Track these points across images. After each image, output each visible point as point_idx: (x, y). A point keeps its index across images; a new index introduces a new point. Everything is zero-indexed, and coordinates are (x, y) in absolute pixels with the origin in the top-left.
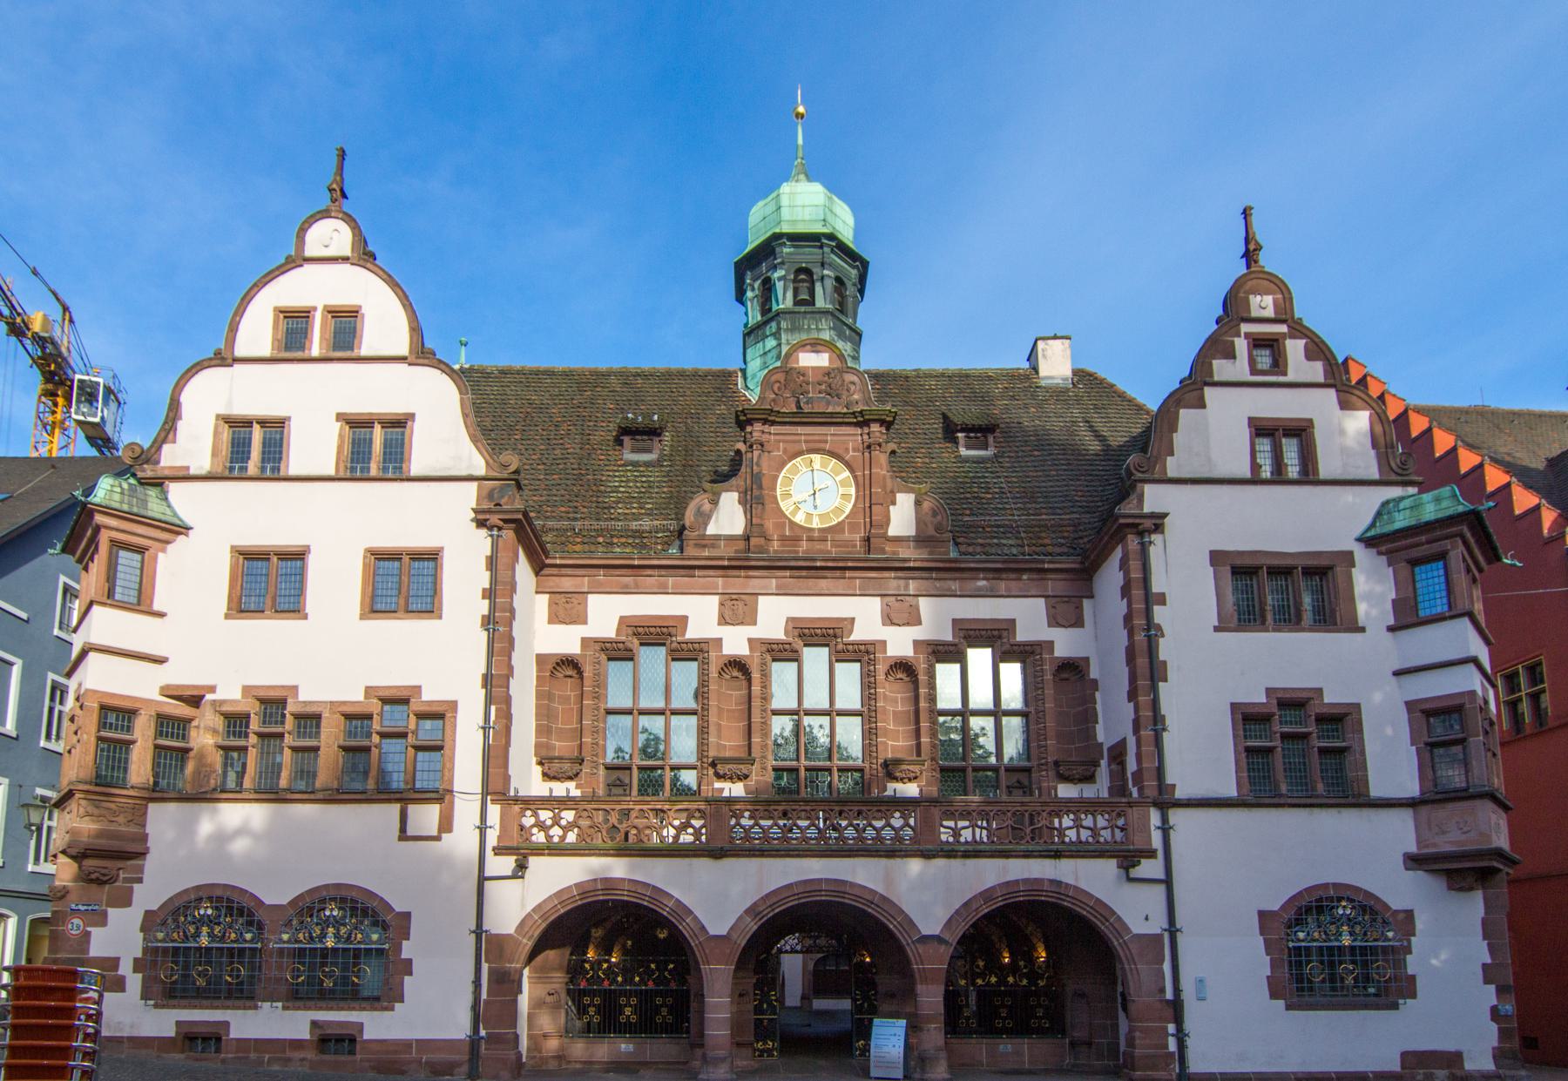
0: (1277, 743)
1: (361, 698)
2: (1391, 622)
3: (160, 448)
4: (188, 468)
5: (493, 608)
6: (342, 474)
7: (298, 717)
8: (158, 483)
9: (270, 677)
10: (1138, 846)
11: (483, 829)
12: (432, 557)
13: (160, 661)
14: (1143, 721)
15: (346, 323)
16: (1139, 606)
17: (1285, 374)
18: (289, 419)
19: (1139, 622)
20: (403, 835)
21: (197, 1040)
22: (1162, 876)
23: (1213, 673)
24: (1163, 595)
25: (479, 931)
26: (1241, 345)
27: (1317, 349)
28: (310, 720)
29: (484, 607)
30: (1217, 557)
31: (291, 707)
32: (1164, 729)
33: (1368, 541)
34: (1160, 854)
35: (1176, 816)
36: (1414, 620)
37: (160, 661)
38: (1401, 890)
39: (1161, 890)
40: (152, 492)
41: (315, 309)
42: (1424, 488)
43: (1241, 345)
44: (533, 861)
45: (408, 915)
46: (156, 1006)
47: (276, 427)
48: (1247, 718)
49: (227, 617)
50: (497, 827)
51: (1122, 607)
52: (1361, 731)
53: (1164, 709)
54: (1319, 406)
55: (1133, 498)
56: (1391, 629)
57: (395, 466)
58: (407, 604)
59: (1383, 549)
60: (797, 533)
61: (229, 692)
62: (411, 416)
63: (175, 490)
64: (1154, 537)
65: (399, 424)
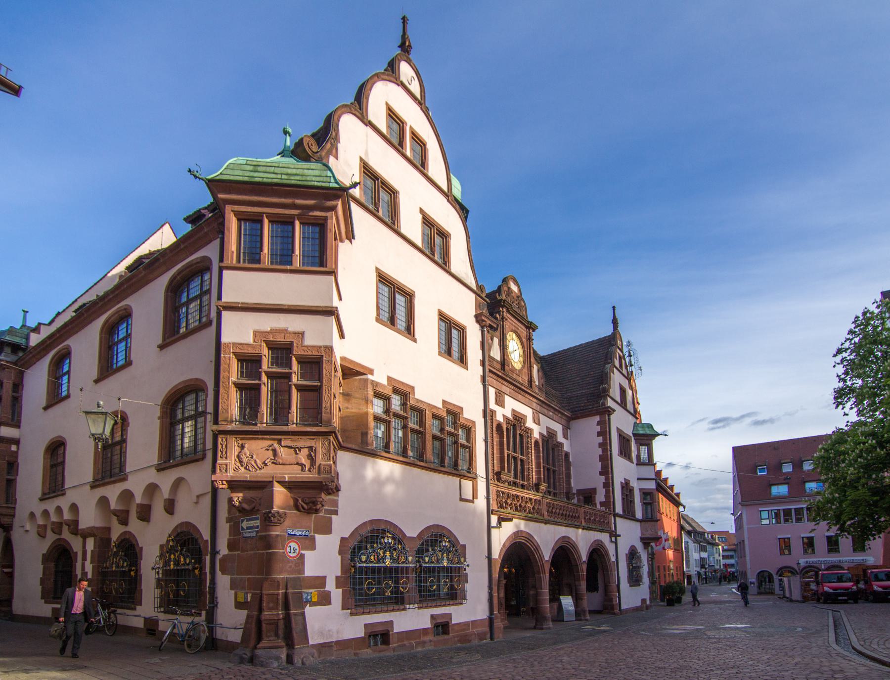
21: (380, 636)
44: (503, 523)
46: (352, 614)
60: (513, 370)
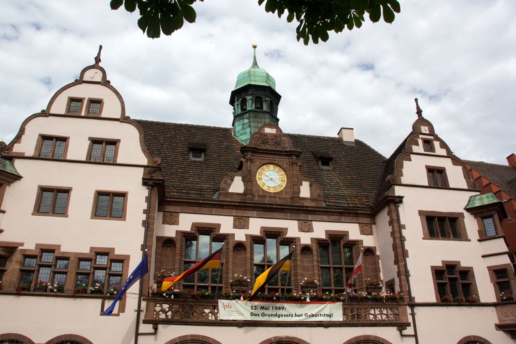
0: (447, 281)
2: (478, 238)
3: (14, 144)
4: (24, 153)
5: (148, 217)
6: (88, 161)
8: (11, 159)
9: (48, 241)
10: (404, 321)
11: (139, 311)
14: (401, 272)
16: (397, 229)
17: (435, 152)
18: (69, 138)
19: (397, 235)
22: (413, 333)
23: (425, 255)
24: (404, 225)
26: (420, 142)
27: (443, 145)
29: (144, 217)
30: (421, 213)
32: (409, 276)
33: (468, 210)
34: (412, 324)
35: (417, 310)
36: (486, 238)
39: (413, 339)
40: (7, 162)
41: (85, 99)
42: (482, 192)
44: (160, 327)
48: (438, 273)
49: (33, 214)
50: (145, 311)
51: (390, 229)
52: (474, 277)
53: (409, 268)
54: (446, 164)
55: (391, 190)
56: (479, 241)
58: (111, 214)
59: (473, 213)
61: (30, 246)
62: (119, 141)
63: (18, 163)
64: (399, 205)
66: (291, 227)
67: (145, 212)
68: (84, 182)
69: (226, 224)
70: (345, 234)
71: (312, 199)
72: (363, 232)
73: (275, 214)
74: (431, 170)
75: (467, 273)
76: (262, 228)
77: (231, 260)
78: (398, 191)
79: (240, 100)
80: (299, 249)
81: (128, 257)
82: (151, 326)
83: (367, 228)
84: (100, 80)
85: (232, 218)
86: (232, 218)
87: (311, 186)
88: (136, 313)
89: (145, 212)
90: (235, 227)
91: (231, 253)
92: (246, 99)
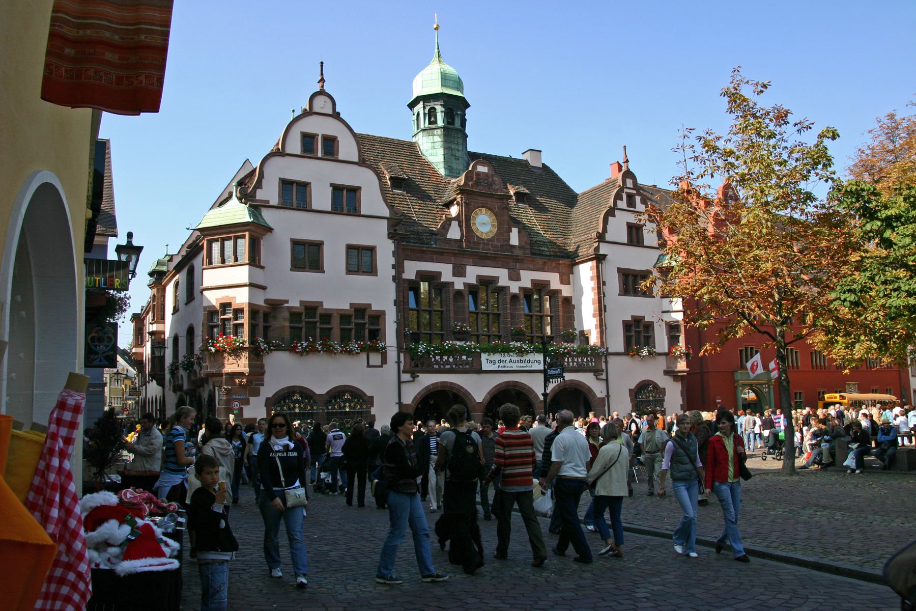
1: (348, 307)
3: (255, 192)
4: (268, 202)
7: (322, 316)
11: (399, 362)
12: (372, 250)
13: (264, 288)
15: (330, 143)
20: (369, 366)
25: (400, 403)
26: (624, 196)
28: (327, 317)
30: (619, 270)
31: (319, 312)
37: (264, 288)
38: (663, 382)
39: (604, 383)
43: (624, 196)
45: (372, 397)
47: (304, 186)
48: (627, 326)
57: (354, 210)
61: (294, 303)
62: (360, 188)
65: (354, 191)
66: (502, 275)
67: (394, 267)
68: (337, 235)
69: (446, 271)
70: (547, 283)
71: (520, 247)
72: (562, 282)
73: (489, 262)
74: (630, 226)
75: (649, 326)
76: (478, 276)
77: (452, 308)
78: (604, 249)
79: (428, 108)
80: (508, 297)
81: (383, 312)
82: (409, 375)
83: (565, 277)
84: (330, 112)
85: (451, 266)
86: (451, 266)
87: (519, 232)
88: (396, 365)
89: (394, 267)
90: (454, 275)
91: (452, 302)
92: (435, 109)
